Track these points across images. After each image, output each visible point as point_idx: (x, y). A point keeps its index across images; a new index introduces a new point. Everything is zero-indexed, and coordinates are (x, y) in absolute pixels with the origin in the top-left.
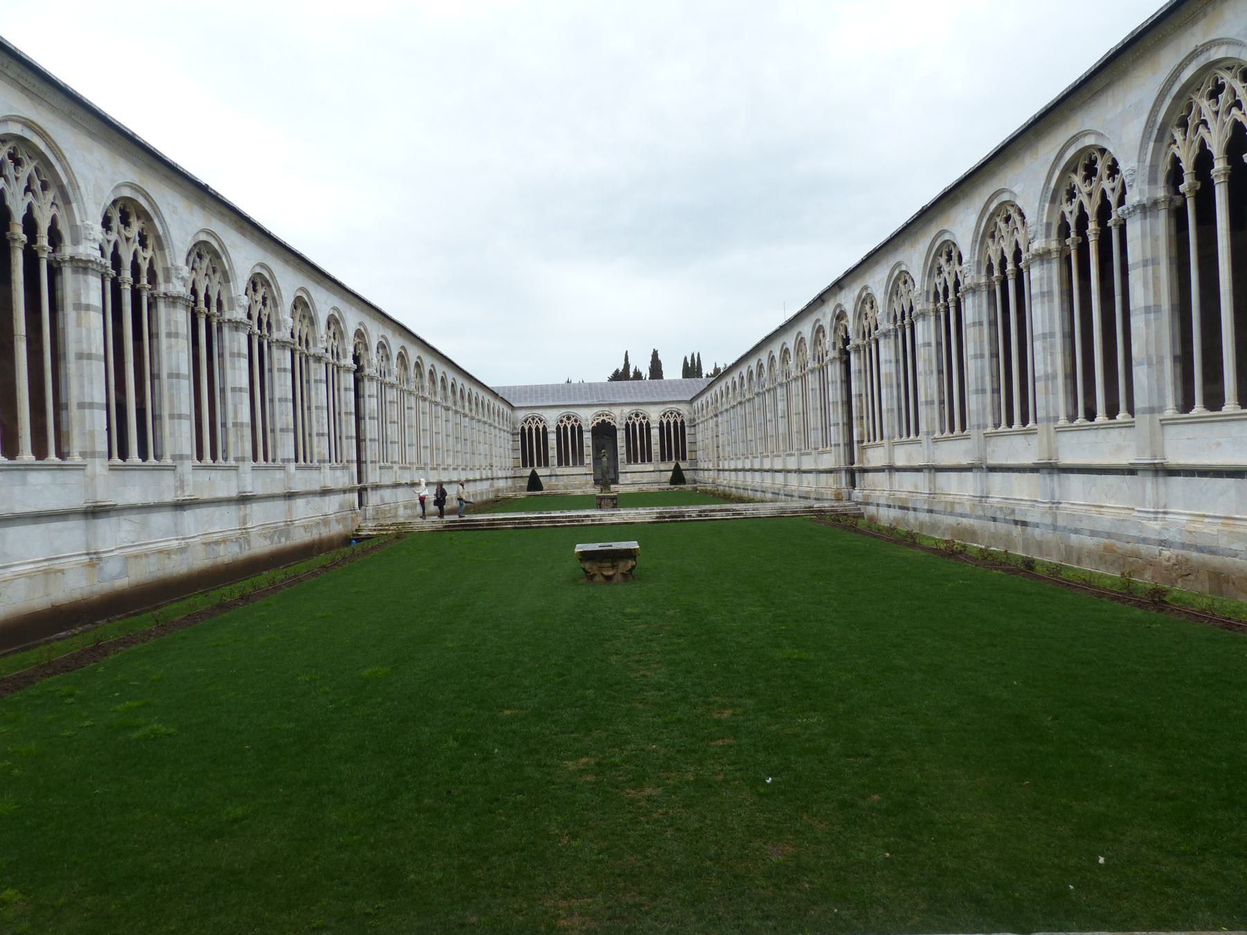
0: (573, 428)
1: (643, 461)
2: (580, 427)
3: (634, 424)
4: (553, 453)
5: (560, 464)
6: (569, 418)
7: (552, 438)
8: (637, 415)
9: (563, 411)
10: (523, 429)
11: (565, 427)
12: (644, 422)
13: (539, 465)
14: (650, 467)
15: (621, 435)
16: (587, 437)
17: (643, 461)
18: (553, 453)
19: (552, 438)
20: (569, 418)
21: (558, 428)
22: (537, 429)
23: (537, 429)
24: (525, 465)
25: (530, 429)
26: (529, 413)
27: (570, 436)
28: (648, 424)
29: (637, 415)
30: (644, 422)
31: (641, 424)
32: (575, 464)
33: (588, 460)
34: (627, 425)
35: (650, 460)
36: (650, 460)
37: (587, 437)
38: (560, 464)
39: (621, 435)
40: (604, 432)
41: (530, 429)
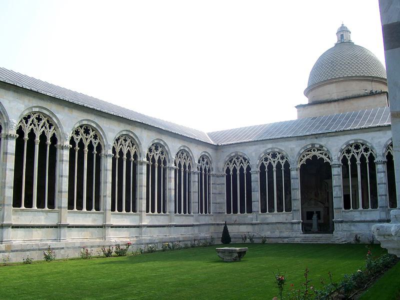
0: (279, 165)
1: (365, 206)
2: (287, 165)
3: (353, 159)
4: (256, 196)
5: (264, 210)
6: (274, 156)
7: (256, 177)
8: (357, 147)
9: (270, 146)
10: (228, 170)
11: (270, 166)
12: (367, 155)
13: (242, 211)
14: (375, 215)
15: (336, 172)
16: (295, 174)
17: (365, 206)
18: (256, 196)
19: (256, 177)
20: (274, 156)
21: (262, 167)
22: (242, 169)
23: (242, 169)
24: (229, 212)
25: (235, 170)
26: (231, 152)
27: (275, 174)
28: (372, 158)
29: (357, 147)
30: (367, 155)
31: (363, 158)
32: (280, 210)
33: (297, 204)
34: (344, 160)
35: (375, 205)
36: (375, 205)
37: (295, 174)
38: (264, 210)
39: (336, 172)
40: (316, 170)
41: (235, 170)
